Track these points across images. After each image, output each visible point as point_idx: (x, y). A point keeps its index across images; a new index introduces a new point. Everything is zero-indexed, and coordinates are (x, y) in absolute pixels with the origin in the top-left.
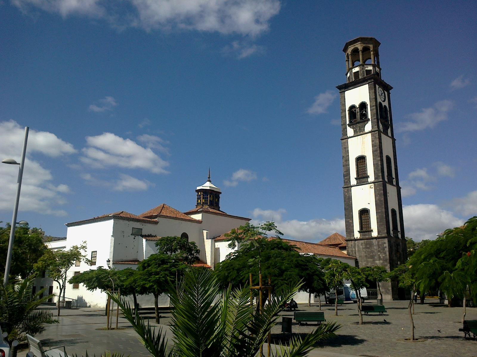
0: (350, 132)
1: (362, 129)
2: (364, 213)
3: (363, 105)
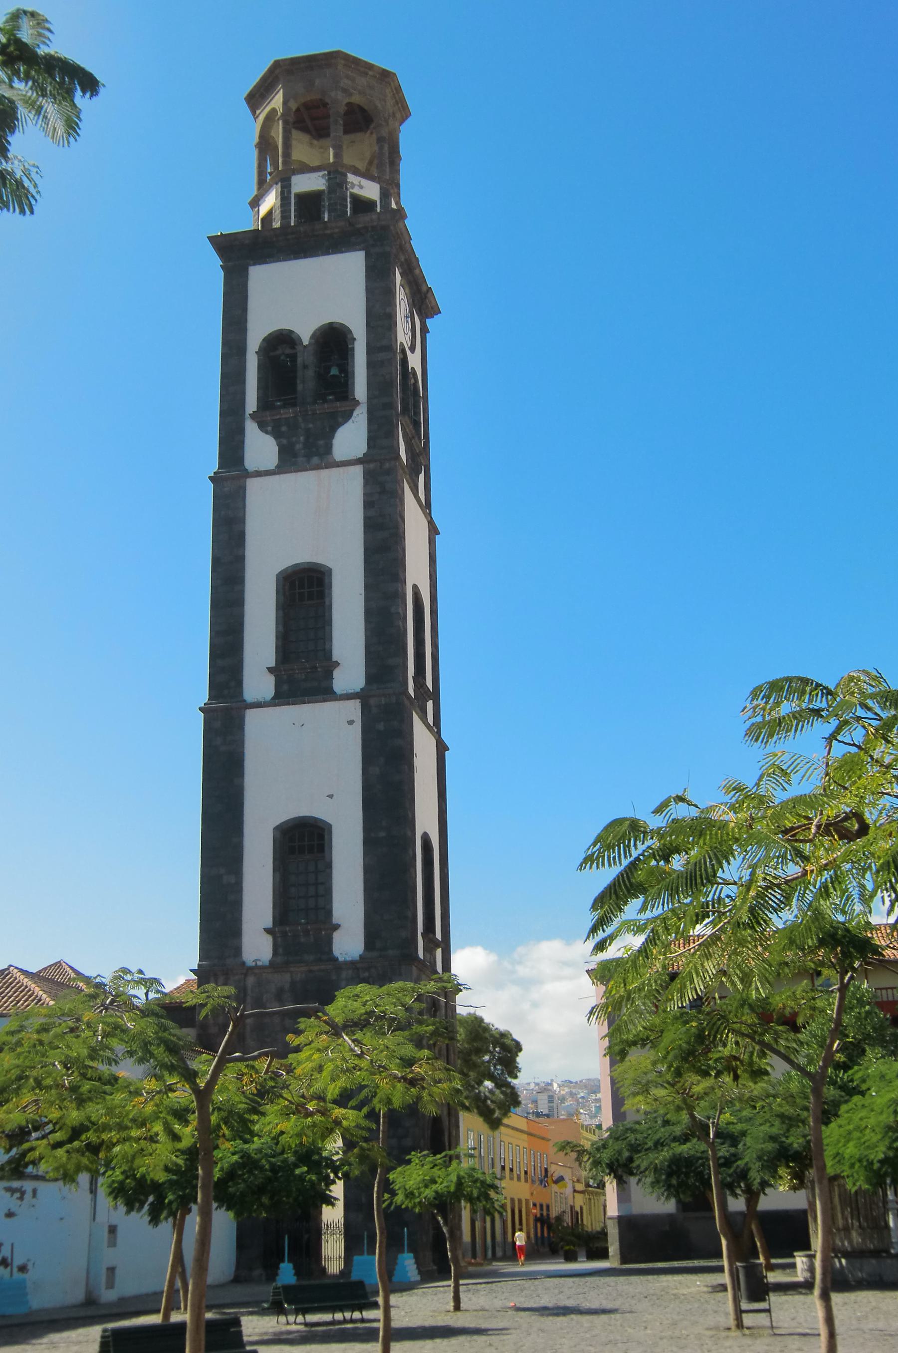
0: (261, 448)
1: (321, 442)
2: (303, 842)
3: (333, 340)
